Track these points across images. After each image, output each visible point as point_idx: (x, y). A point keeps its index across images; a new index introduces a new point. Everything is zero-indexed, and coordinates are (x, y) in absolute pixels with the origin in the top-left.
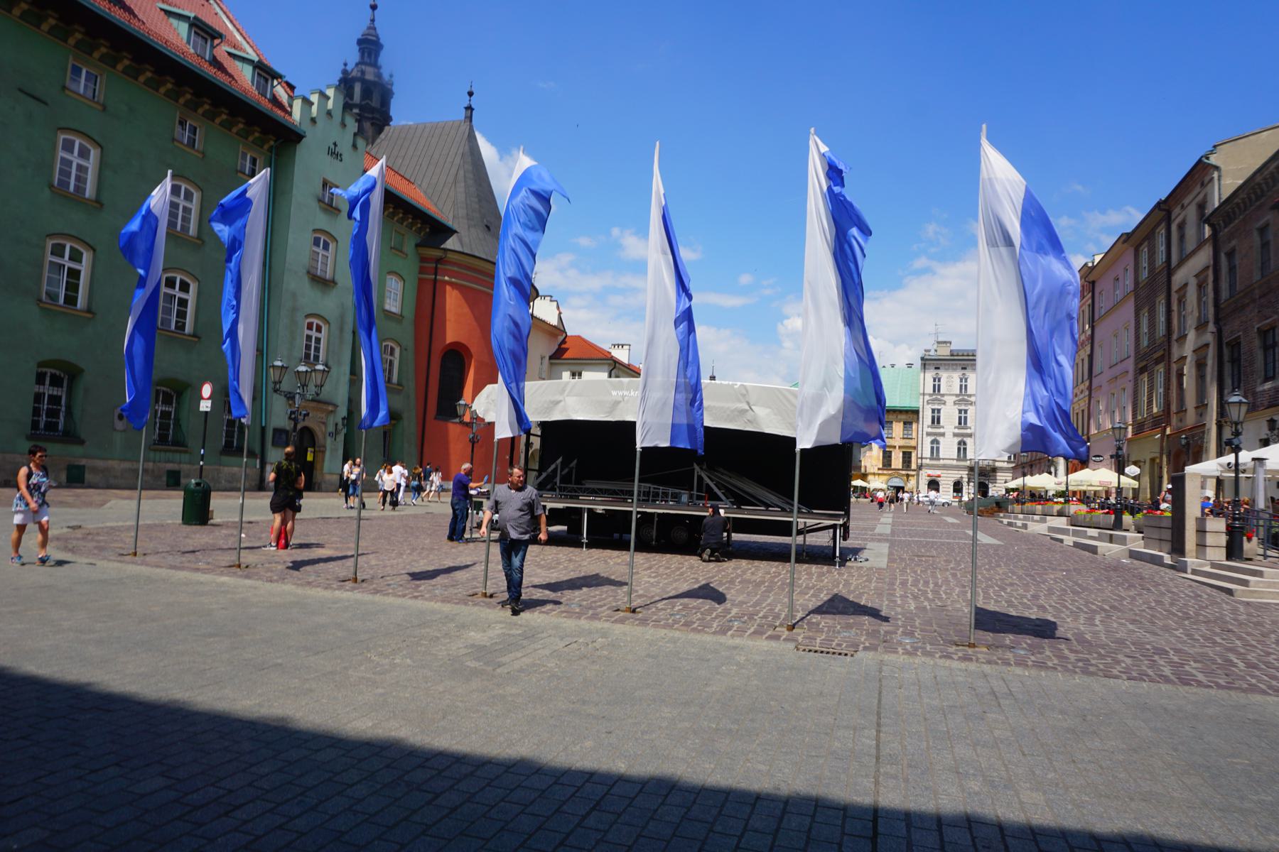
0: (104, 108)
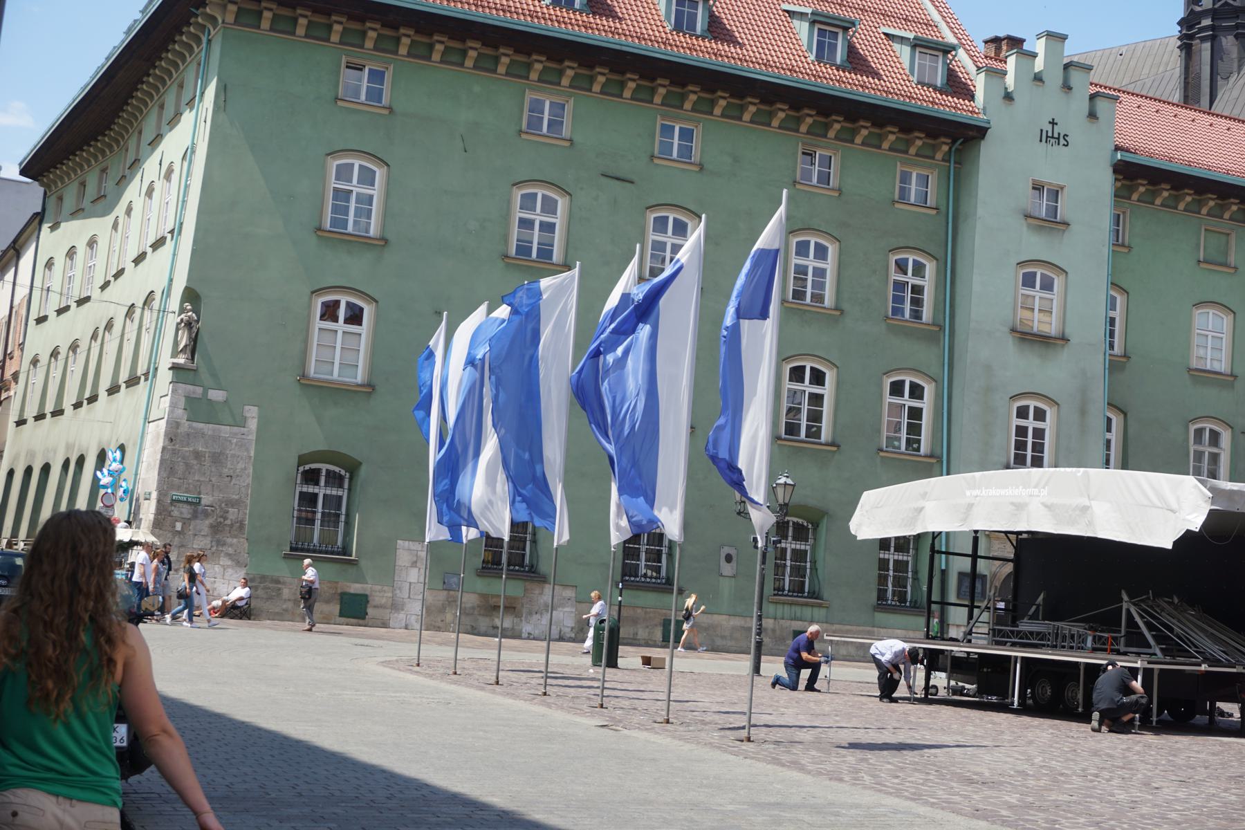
0: (701, 167)
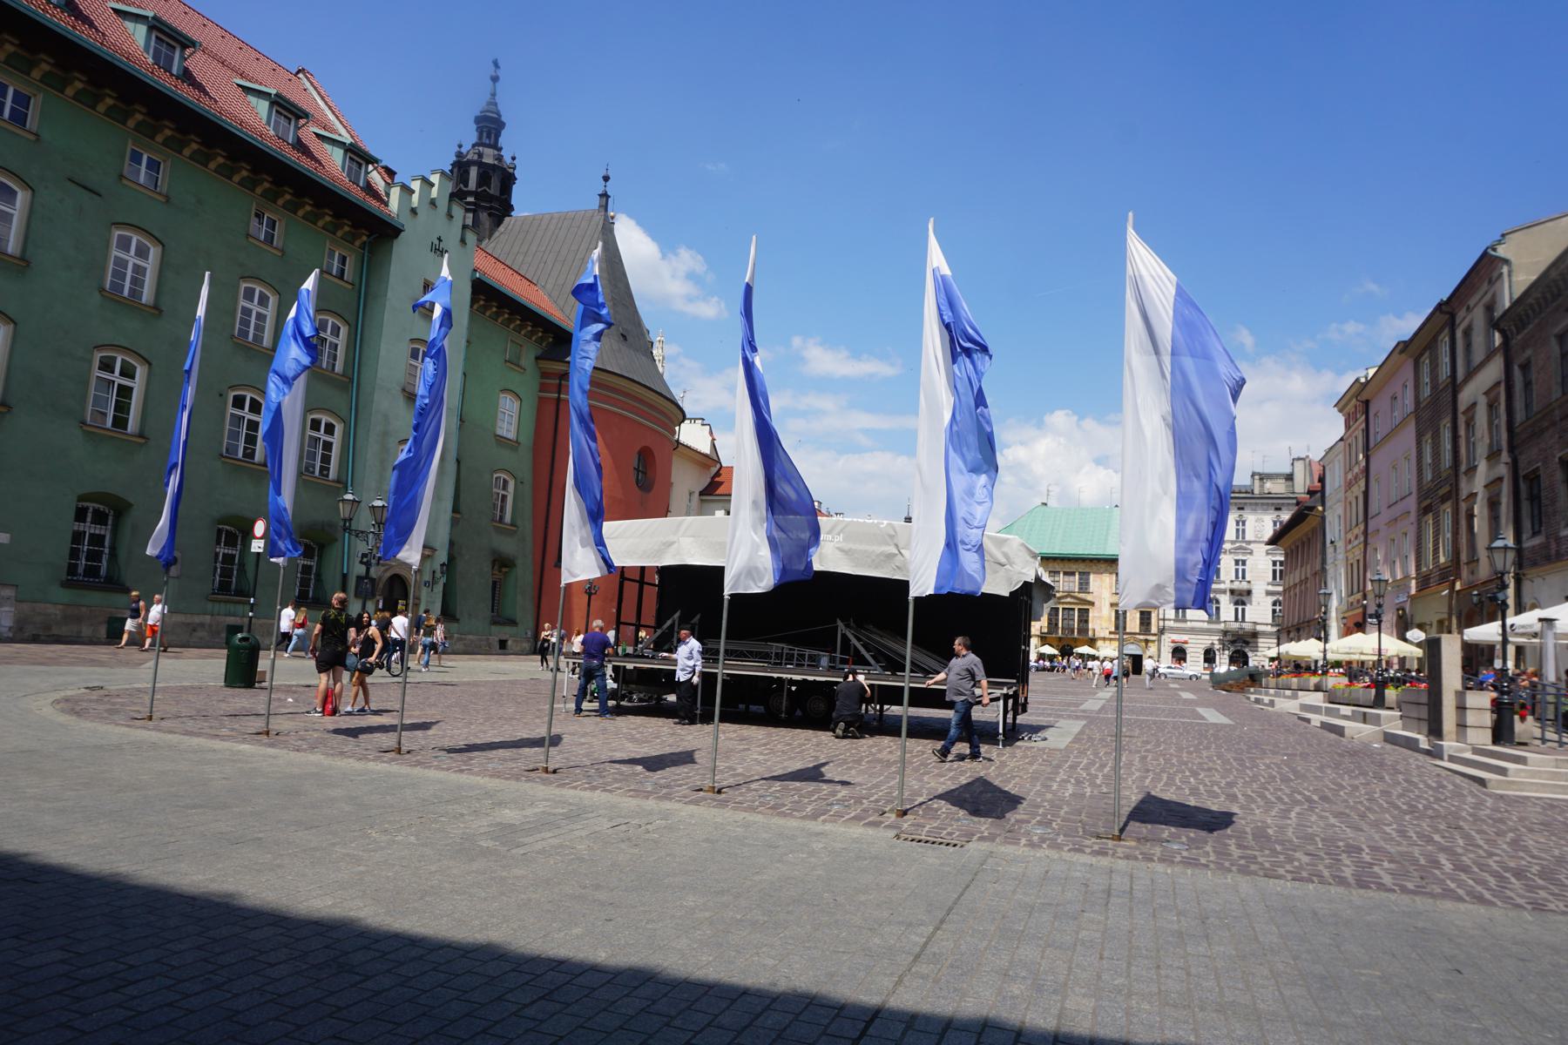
0: (168, 199)
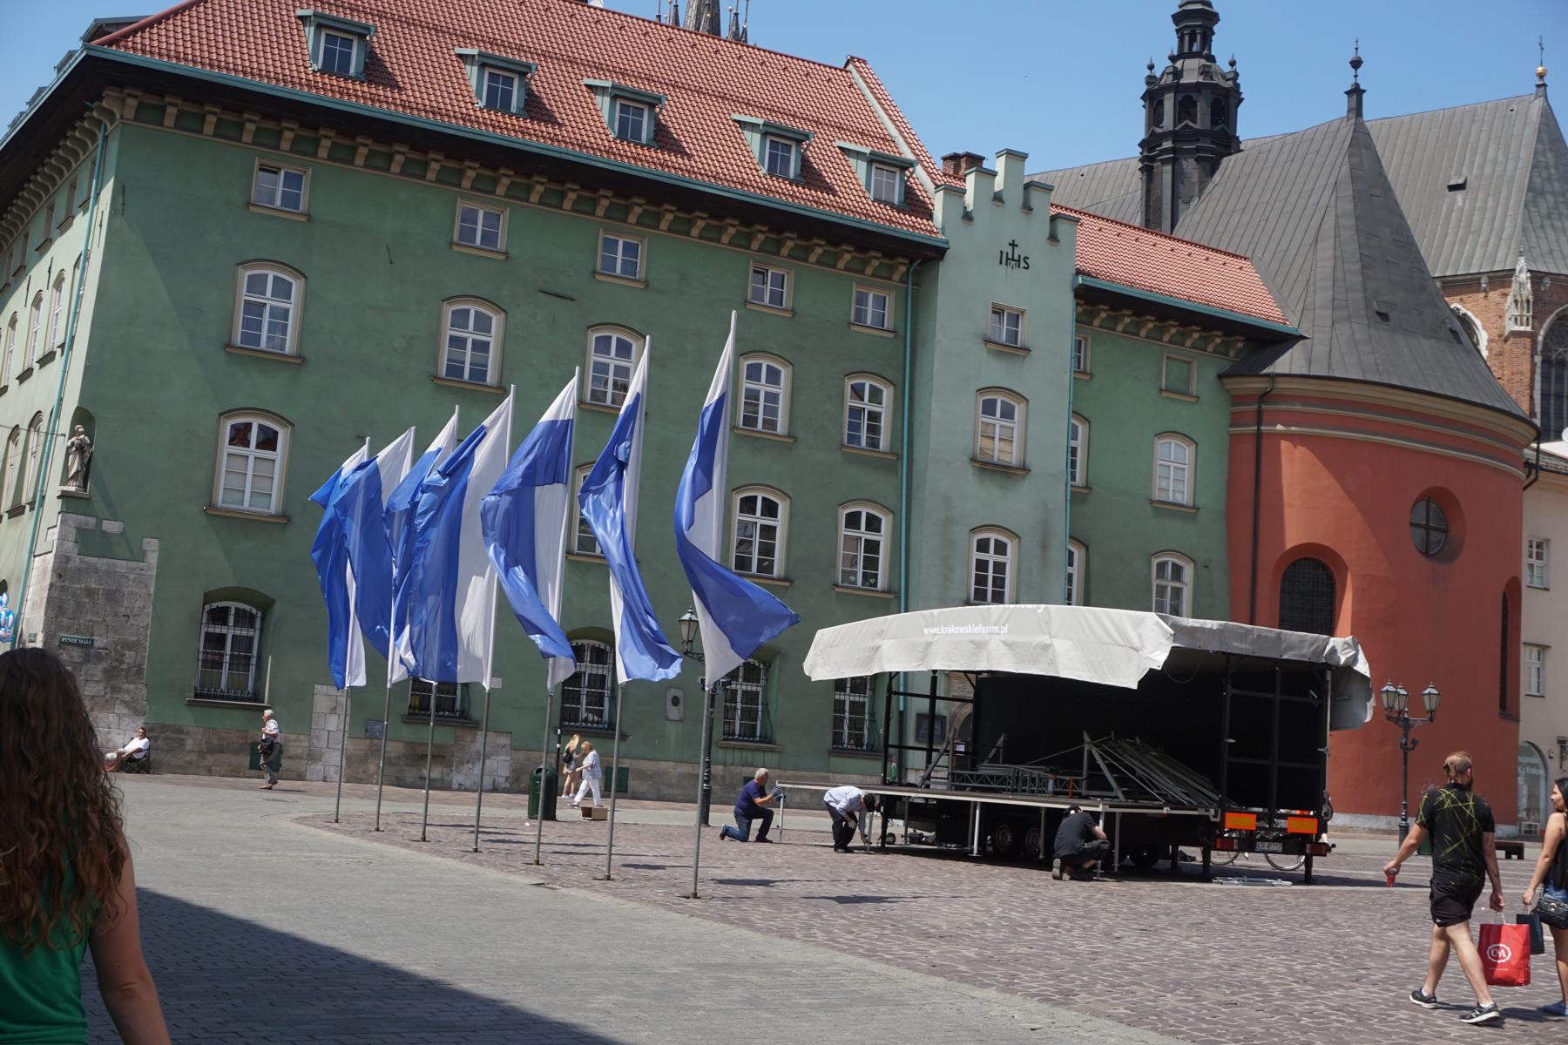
0: (646, 284)
